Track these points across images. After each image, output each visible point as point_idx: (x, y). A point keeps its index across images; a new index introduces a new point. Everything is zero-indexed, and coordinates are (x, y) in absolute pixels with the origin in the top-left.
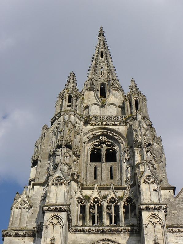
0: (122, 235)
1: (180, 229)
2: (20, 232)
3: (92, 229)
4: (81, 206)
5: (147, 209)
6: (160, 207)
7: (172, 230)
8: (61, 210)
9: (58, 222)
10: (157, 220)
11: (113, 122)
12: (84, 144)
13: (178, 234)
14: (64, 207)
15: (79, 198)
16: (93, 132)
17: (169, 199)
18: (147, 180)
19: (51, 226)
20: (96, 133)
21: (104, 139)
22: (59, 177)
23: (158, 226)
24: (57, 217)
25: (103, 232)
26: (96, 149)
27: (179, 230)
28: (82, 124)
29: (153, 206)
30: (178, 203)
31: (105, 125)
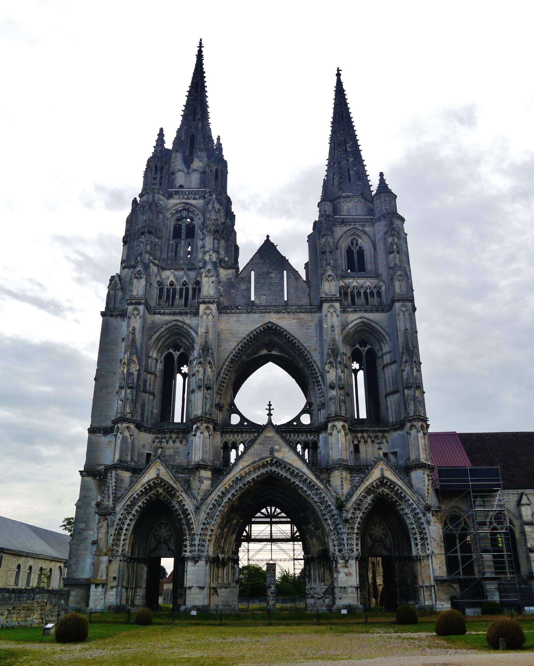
0: (189, 316)
1: (232, 311)
2: (113, 313)
3: (167, 311)
4: (160, 289)
5: (204, 302)
6: (213, 301)
7: (226, 312)
8: (140, 304)
9: (138, 314)
10: (210, 311)
11: (193, 196)
12: (167, 221)
13: (231, 315)
14: (142, 301)
15: (158, 281)
16: (176, 208)
17: (231, 279)
18: (208, 274)
19: (132, 317)
20: (178, 208)
21: (184, 214)
22: (139, 271)
23: (210, 317)
24: (136, 309)
25: (174, 314)
26: (177, 224)
27: (231, 312)
28: (166, 199)
29: (207, 300)
30: (237, 283)
31: (186, 199)
